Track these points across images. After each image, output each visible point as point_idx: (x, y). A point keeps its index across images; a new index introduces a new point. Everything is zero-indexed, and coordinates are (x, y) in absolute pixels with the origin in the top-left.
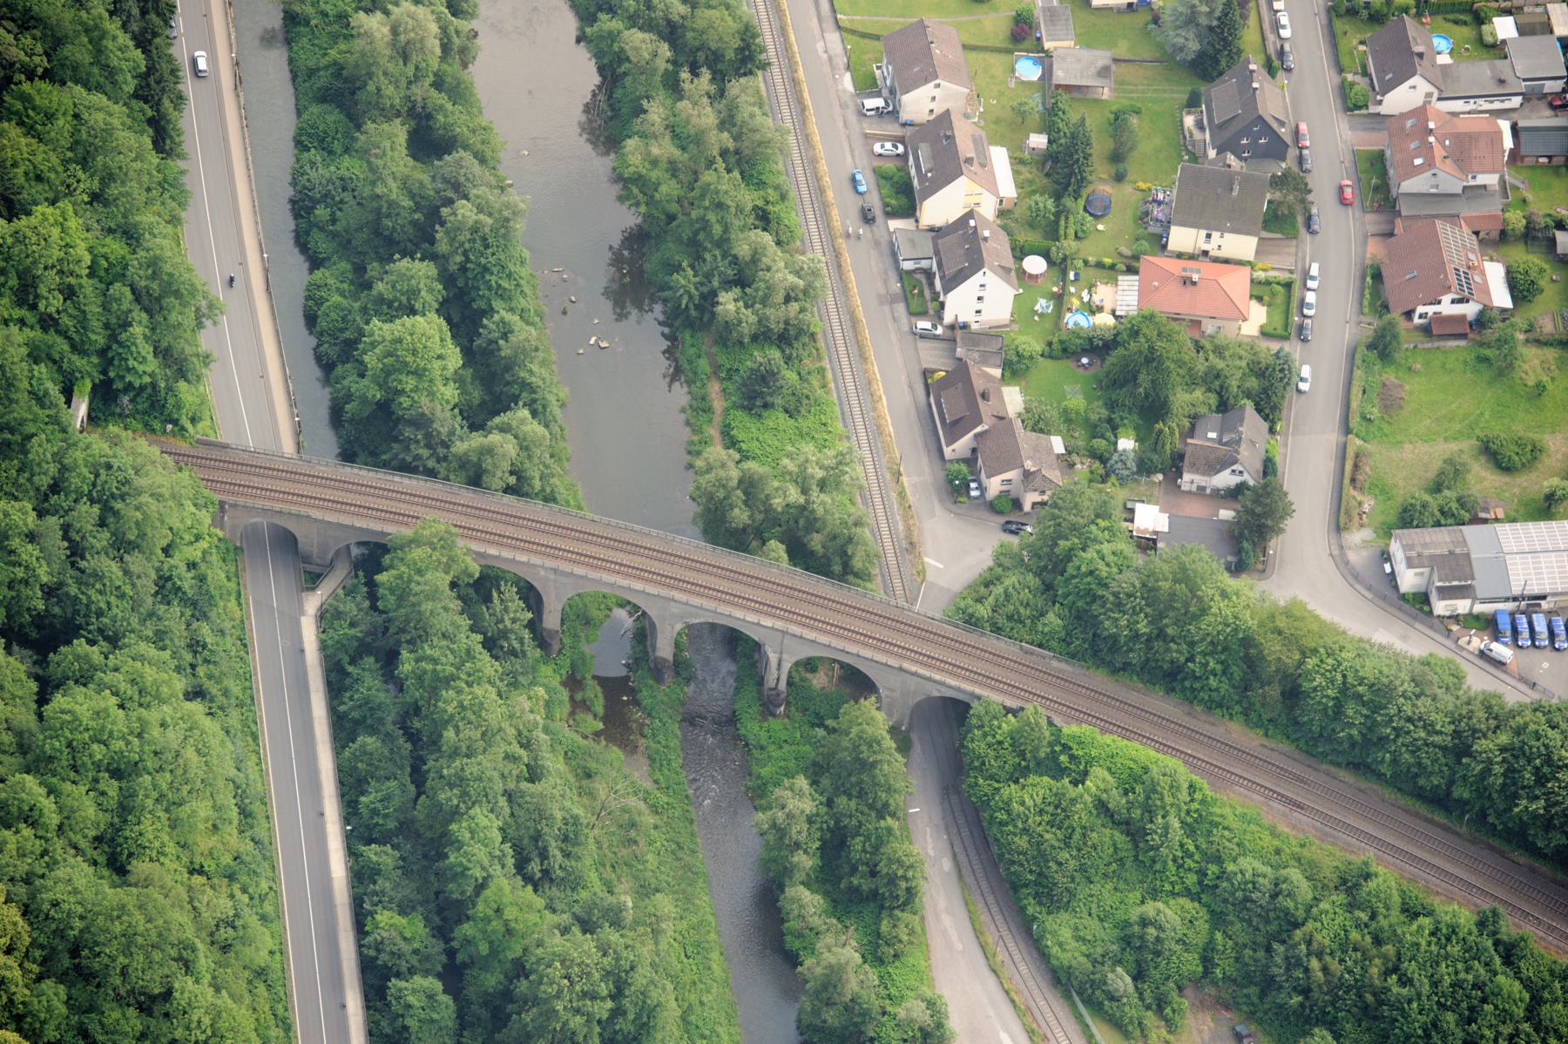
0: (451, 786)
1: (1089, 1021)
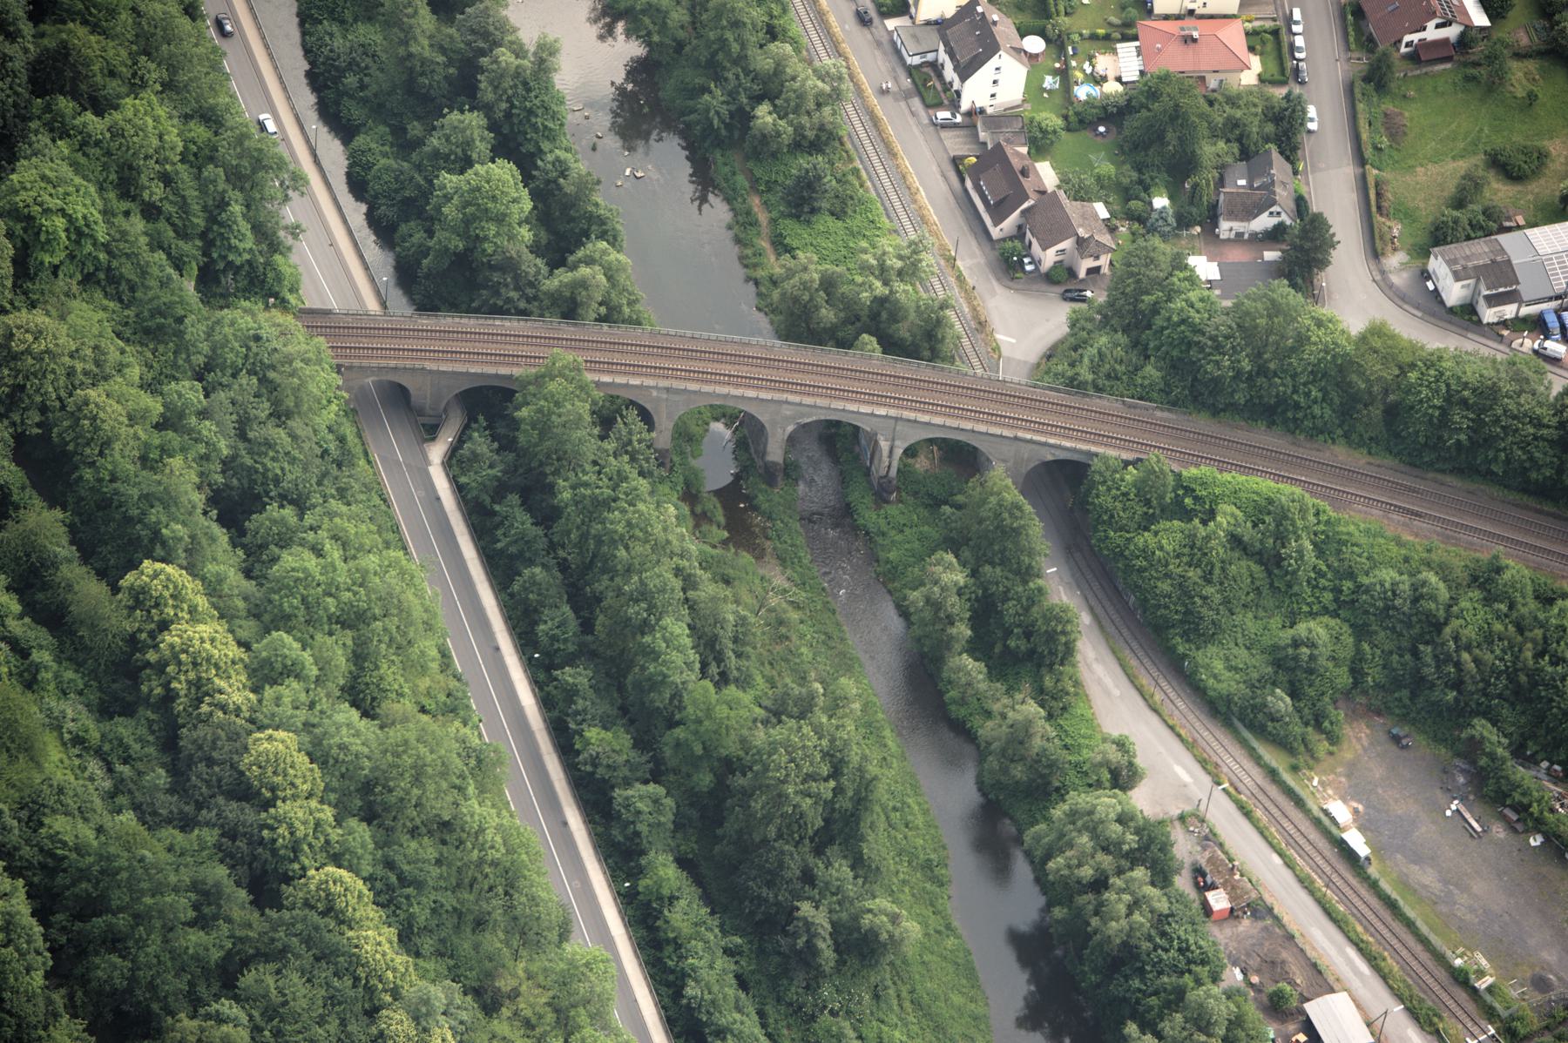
0: (637, 601)
1: (1255, 744)
